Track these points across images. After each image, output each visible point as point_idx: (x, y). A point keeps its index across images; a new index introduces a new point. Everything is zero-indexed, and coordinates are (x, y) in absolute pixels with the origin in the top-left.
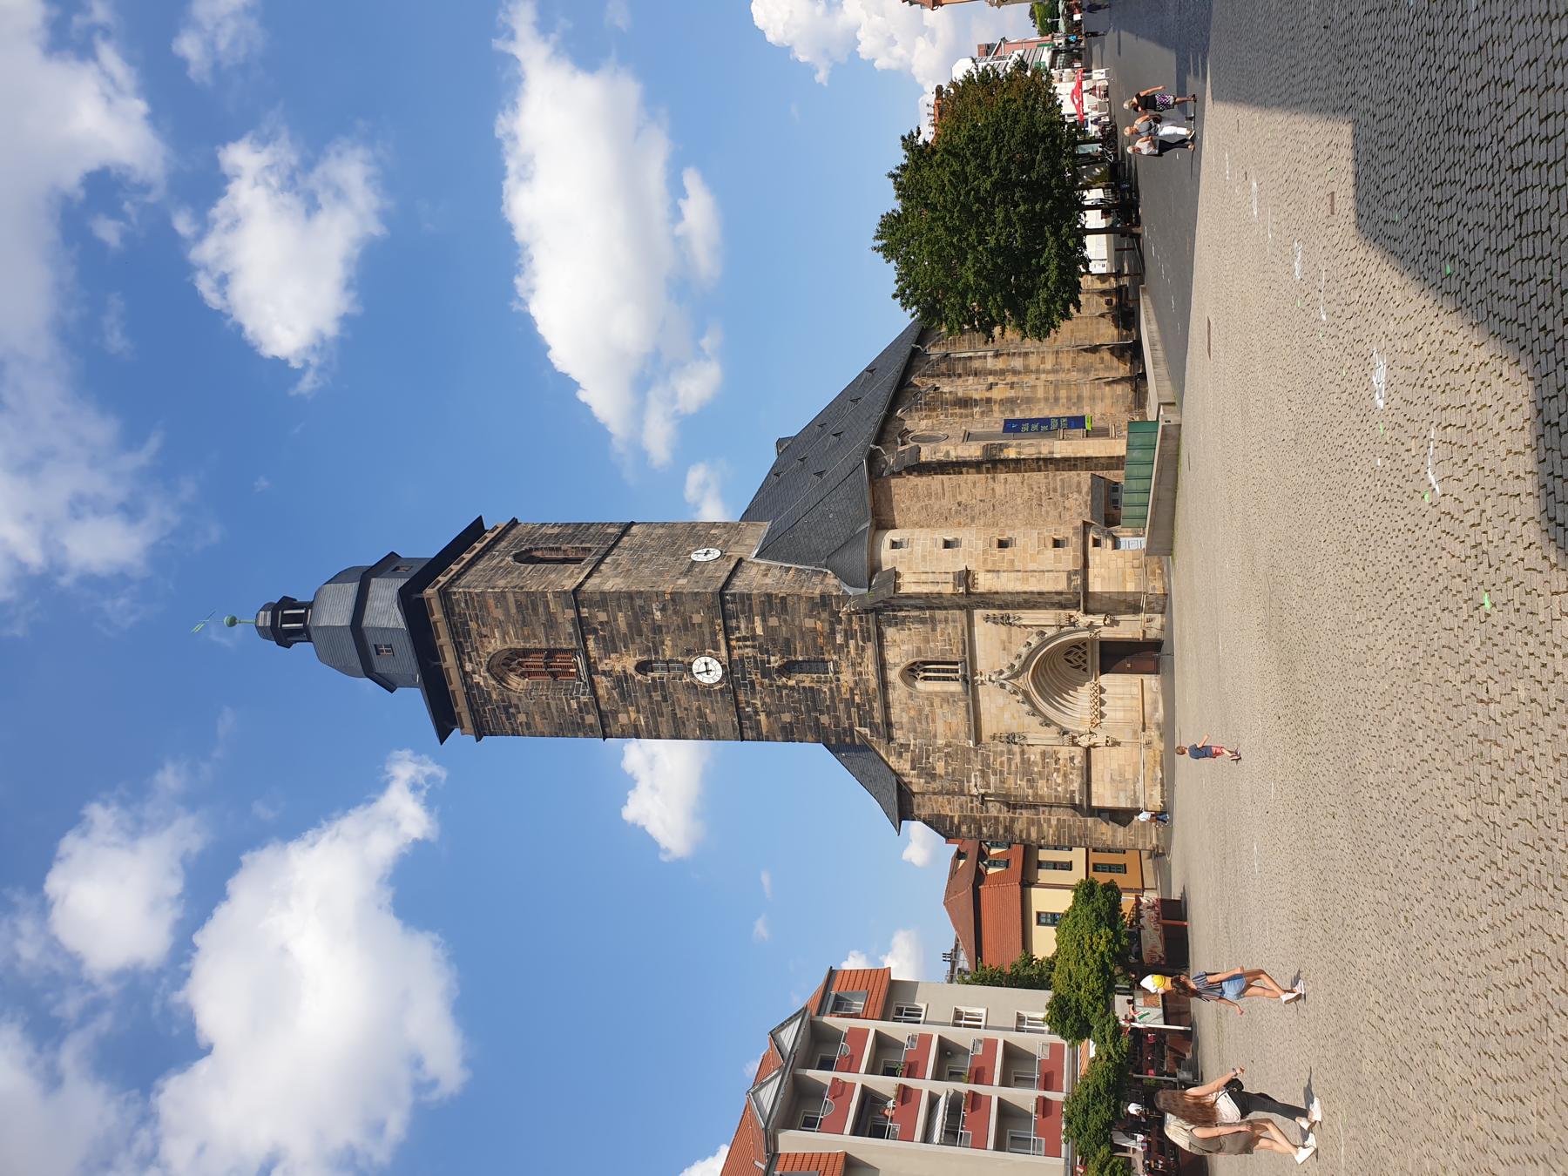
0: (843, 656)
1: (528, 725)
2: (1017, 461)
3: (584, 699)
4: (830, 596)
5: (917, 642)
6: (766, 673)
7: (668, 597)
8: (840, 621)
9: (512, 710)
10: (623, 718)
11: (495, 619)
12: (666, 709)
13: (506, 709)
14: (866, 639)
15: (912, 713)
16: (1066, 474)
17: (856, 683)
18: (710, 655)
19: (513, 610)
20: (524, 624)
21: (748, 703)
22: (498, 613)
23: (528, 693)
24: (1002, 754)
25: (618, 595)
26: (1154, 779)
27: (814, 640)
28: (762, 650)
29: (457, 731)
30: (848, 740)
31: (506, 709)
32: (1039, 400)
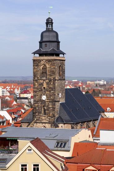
3: (39, 78)
6: (44, 106)
10: (36, 83)
12: (38, 90)
19: (53, 70)
22: (52, 67)
23: (40, 69)
25: (55, 86)
28: (47, 106)
31: (37, 65)
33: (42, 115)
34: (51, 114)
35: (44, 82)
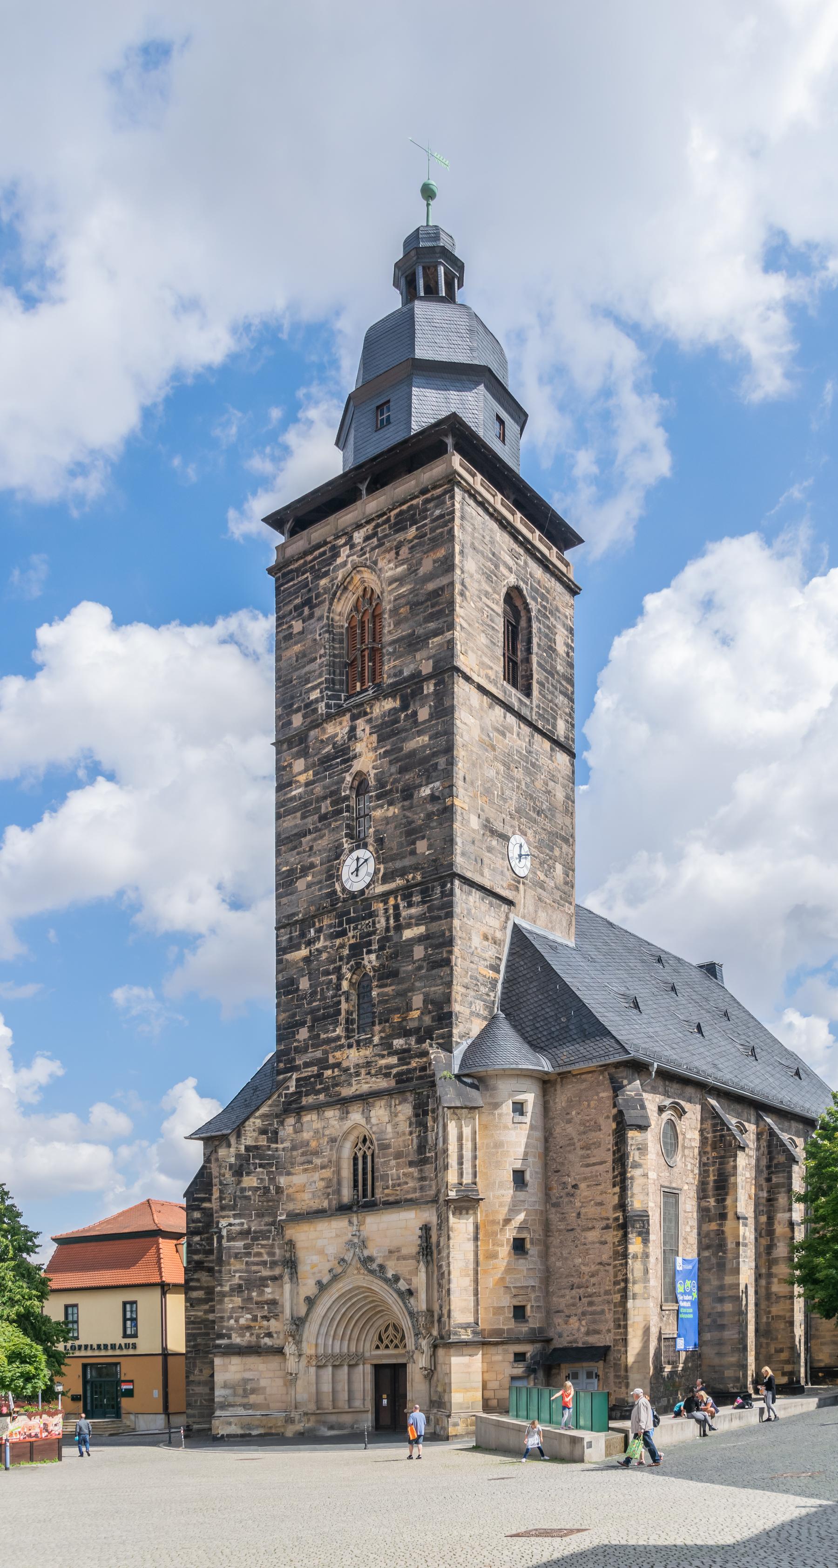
0: (377, 1050)
1: (289, 637)
2: (625, 1255)
3: (322, 708)
4: (450, 1025)
5: (396, 1143)
6: (356, 950)
7: (448, 801)
8: (420, 1041)
9: (306, 610)
10: (299, 765)
11: (419, 563)
12: (311, 821)
13: (308, 602)
14: (401, 1079)
15: (313, 1144)
16: (609, 1316)
17: (348, 1069)
18: (377, 871)
19: (431, 586)
20: (414, 605)
21: (319, 930)
22: (427, 566)
23: (330, 628)
24: (271, 1254)
25: (448, 733)
26: (249, 1426)
27: (397, 1010)
28: (384, 941)
29: (281, 539)
30: (282, 1065)
32: (721, 1278)
33: (339, 1031)
34: (417, 1000)
35: (361, 723)
